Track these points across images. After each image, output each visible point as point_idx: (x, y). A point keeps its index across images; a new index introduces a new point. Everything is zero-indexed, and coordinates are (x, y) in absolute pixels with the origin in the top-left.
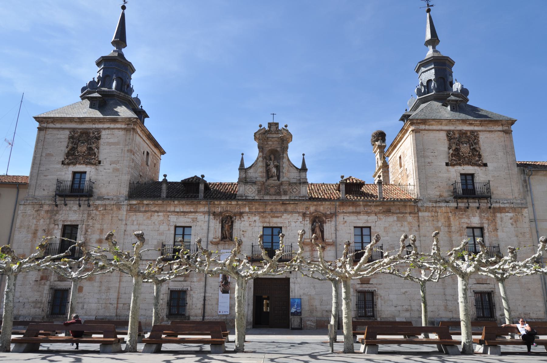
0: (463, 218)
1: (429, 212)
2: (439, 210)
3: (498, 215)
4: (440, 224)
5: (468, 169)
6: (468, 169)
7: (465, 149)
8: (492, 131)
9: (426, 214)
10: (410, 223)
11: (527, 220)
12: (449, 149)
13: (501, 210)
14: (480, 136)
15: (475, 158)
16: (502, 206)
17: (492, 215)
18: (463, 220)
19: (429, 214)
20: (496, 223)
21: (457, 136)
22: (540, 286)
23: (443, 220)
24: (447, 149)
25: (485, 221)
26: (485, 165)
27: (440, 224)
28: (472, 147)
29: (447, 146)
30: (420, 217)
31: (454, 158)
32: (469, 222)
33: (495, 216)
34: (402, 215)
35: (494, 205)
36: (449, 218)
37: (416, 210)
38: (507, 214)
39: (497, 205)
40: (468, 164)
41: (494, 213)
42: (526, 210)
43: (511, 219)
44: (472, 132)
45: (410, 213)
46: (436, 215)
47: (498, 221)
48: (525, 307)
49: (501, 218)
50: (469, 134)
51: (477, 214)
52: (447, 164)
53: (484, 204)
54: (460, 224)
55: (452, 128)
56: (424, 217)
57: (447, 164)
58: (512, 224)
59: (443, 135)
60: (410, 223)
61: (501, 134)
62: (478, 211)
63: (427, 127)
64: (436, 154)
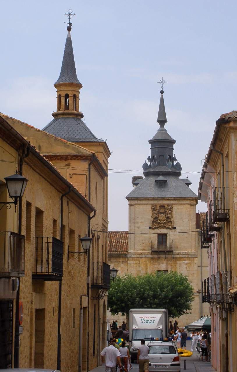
0: (156, 264)
1: (134, 260)
2: (141, 260)
3: (178, 262)
4: (140, 269)
5: (163, 231)
6: (163, 231)
7: (162, 217)
8: (182, 204)
9: (132, 262)
10: (122, 268)
11: (196, 265)
12: (152, 217)
13: (180, 259)
14: (174, 208)
15: (169, 224)
16: (181, 256)
17: (174, 262)
18: (155, 266)
19: (135, 262)
20: (176, 267)
21: (158, 208)
22: (199, 307)
23: (142, 266)
24: (150, 217)
25: (169, 267)
26: (175, 228)
27: (140, 269)
28: (166, 216)
29: (151, 215)
30: (128, 265)
31: (155, 224)
32: (159, 267)
33: (176, 263)
34: (117, 263)
35: (175, 256)
36: (146, 265)
37: (127, 260)
38: (184, 262)
39: (178, 256)
40: (163, 227)
41: (176, 261)
42: (197, 258)
43: (186, 265)
44: (168, 205)
45: (123, 262)
46: (139, 262)
47: (178, 266)
48: (187, 320)
49: (180, 264)
50: (166, 206)
51: (165, 262)
52: (150, 228)
53: (169, 256)
54: (153, 269)
55: (155, 202)
56: (130, 264)
57: (150, 228)
58: (186, 268)
59: (149, 208)
60: (122, 268)
61: (189, 206)
62: (166, 260)
63: (139, 202)
64: (143, 221)
